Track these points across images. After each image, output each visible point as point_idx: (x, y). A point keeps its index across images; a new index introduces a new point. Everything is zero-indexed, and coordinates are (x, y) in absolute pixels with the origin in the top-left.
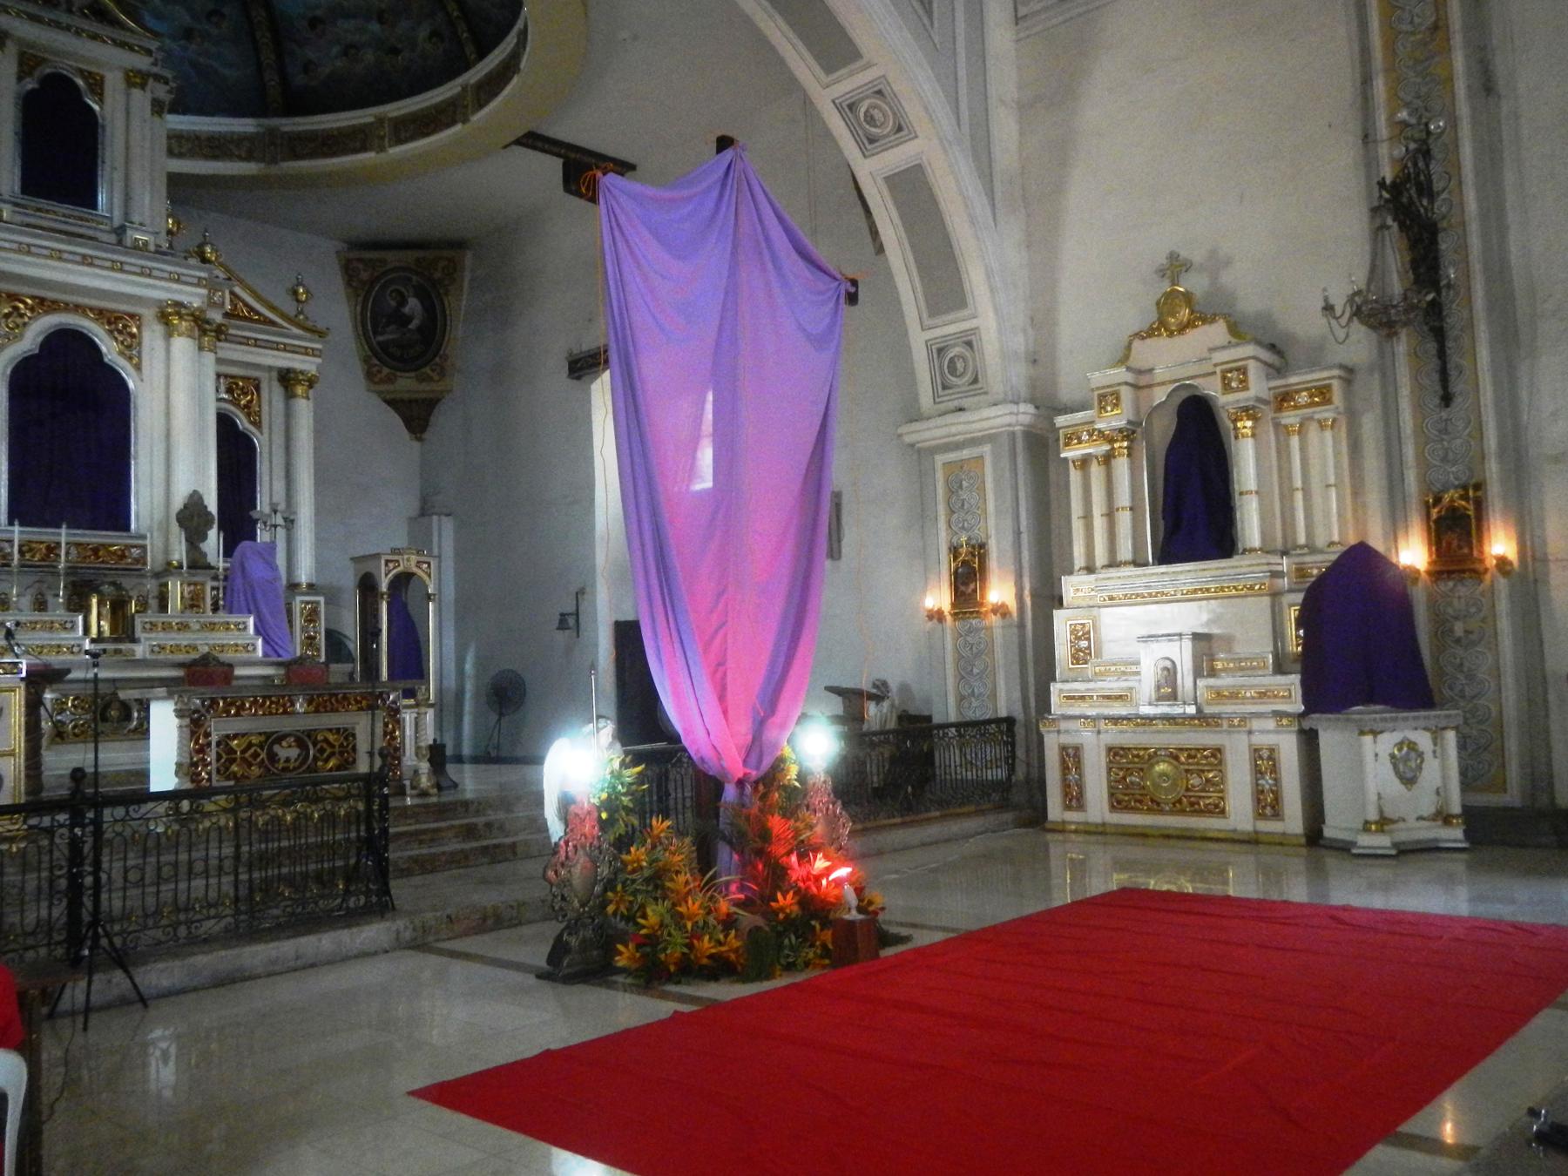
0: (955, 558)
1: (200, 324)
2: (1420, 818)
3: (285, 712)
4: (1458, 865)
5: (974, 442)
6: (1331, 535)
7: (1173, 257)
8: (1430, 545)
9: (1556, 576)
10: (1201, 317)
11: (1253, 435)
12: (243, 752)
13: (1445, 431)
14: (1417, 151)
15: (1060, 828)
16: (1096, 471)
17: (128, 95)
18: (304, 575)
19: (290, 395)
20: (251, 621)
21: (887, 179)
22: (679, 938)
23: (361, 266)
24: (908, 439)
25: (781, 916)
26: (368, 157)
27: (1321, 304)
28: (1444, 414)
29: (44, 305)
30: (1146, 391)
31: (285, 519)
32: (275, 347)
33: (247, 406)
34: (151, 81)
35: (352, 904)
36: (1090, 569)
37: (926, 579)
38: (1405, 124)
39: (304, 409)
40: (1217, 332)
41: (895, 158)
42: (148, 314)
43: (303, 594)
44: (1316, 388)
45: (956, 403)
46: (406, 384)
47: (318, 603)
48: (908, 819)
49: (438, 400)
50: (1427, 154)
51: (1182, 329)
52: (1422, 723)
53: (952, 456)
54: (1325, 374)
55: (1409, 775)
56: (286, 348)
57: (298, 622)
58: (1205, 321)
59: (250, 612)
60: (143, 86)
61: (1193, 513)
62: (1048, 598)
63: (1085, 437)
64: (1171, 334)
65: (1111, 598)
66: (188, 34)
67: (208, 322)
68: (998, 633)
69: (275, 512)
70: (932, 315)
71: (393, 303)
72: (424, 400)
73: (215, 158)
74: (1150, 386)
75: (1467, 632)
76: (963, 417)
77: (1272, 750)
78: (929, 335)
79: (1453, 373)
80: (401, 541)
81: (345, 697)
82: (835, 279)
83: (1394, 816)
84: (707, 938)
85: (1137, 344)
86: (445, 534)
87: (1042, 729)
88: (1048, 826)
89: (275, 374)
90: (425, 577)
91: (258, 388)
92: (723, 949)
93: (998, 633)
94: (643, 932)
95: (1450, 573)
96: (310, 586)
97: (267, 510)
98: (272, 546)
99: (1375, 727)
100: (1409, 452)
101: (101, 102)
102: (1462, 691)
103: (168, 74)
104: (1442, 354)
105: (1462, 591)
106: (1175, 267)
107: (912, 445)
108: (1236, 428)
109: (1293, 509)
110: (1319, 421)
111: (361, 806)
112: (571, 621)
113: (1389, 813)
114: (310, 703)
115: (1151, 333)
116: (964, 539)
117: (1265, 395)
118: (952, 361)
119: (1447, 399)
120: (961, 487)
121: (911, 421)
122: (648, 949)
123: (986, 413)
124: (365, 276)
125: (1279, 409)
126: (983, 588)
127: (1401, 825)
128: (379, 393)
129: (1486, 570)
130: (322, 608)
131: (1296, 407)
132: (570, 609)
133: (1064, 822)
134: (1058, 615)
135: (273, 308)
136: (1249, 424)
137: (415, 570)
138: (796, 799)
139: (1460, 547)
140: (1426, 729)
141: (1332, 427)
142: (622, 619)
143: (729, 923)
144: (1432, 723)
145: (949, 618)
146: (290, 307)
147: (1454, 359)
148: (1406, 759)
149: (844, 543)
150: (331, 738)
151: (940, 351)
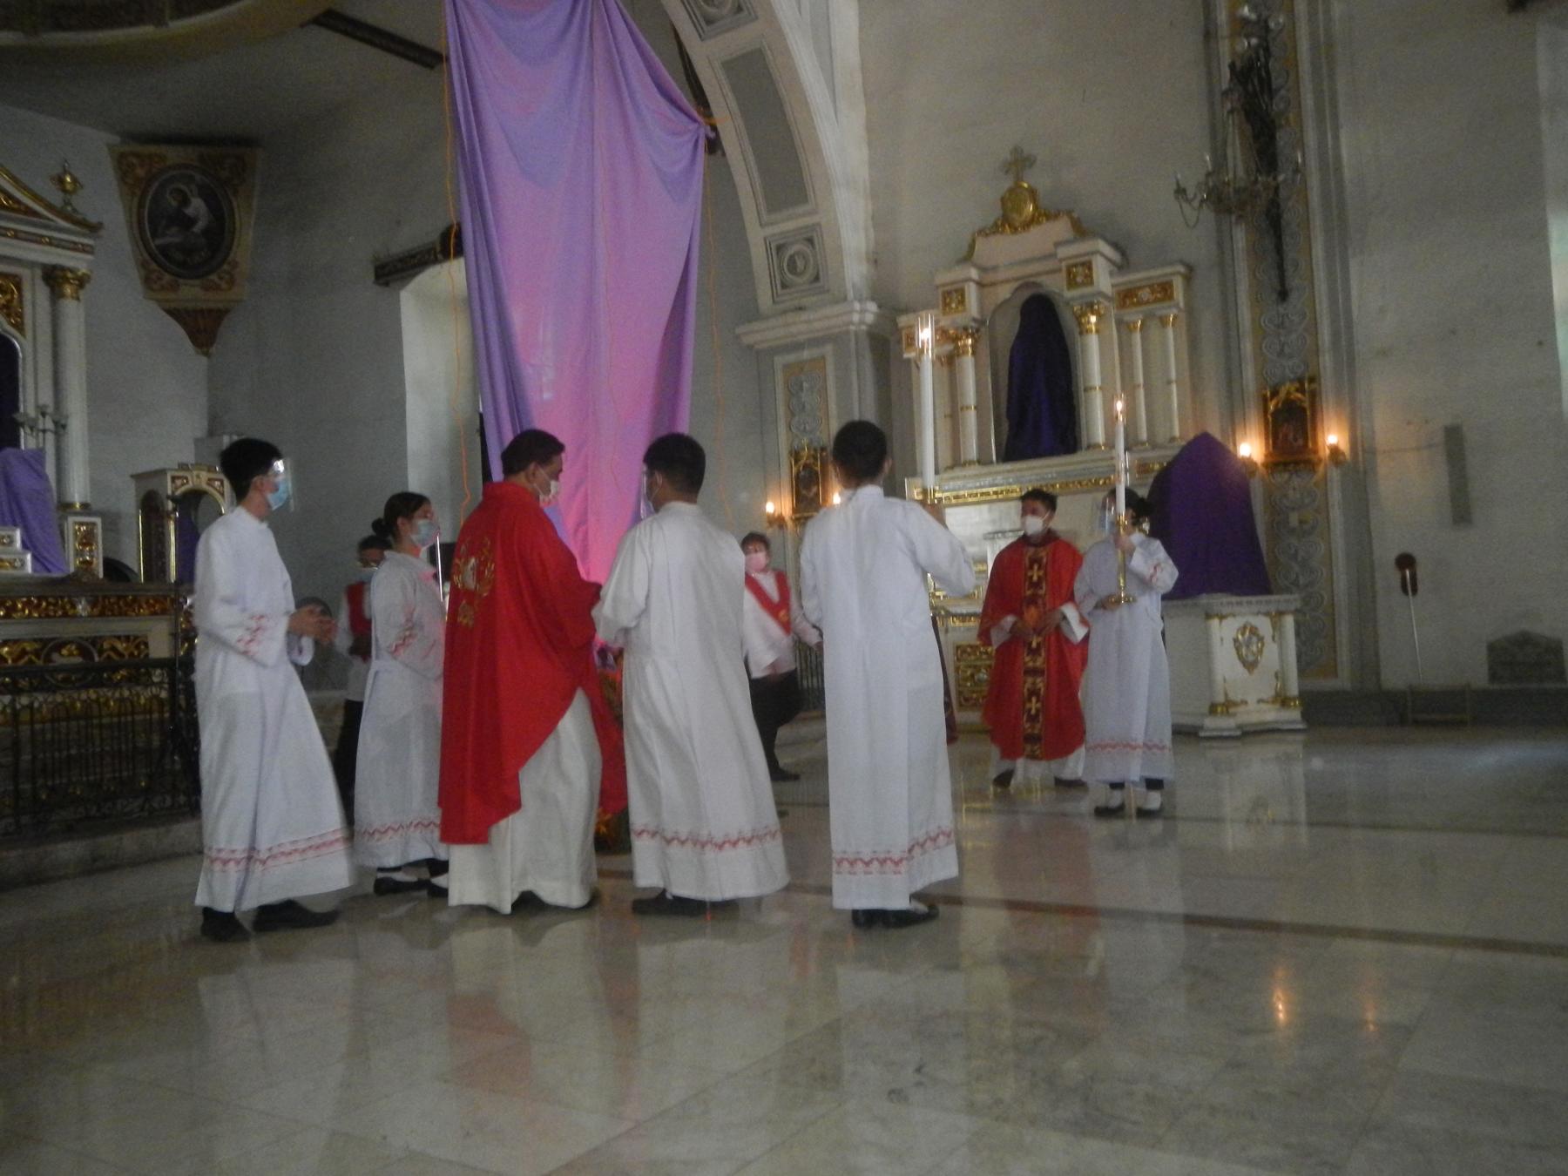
0: (796, 461)
2: (1260, 701)
3: (65, 615)
4: (1294, 746)
6: (1171, 428)
7: (1016, 150)
8: (1267, 439)
9: (1384, 468)
10: (1045, 215)
13: (1281, 325)
14: (1259, 46)
18: (78, 492)
19: (56, 295)
20: (18, 535)
23: (135, 161)
24: (747, 340)
26: (148, 30)
28: (1281, 310)
30: (986, 290)
31: (56, 423)
32: (37, 239)
35: (156, 805)
38: (1245, 21)
39: (73, 311)
43: (76, 514)
45: (796, 303)
46: (191, 293)
47: (94, 524)
49: (227, 311)
50: (1267, 50)
51: (1027, 225)
52: (1264, 608)
53: (791, 358)
54: (1168, 270)
55: (1251, 658)
56: (52, 242)
57: (72, 545)
59: (15, 525)
64: (1015, 230)
65: (957, 497)
69: (44, 415)
70: (770, 211)
71: (174, 203)
72: (210, 311)
74: (993, 284)
75: (1301, 522)
76: (804, 316)
78: (769, 231)
80: (190, 458)
81: (135, 600)
82: (695, 121)
83: (1238, 698)
85: (980, 244)
89: (39, 272)
90: (218, 496)
95: (1286, 464)
96: (85, 506)
97: (32, 412)
98: (39, 455)
99: (1225, 611)
100: (1248, 347)
104: (1279, 250)
105: (1296, 481)
106: (1019, 162)
107: (750, 347)
108: (1080, 324)
111: (164, 694)
113: (1232, 696)
114: (93, 605)
115: (996, 229)
116: (805, 441)
118: (792, 260)
119: (1283, 295)
121: (750, 321)
123: (828, 311)
124: (140, 172)
126: (825, 492)
127: (1241, 709)
128: (158, 301)
129: (1320, 460)
130: (99, 531)
131: (1140, 303)
135: (36, 197)
137: (205, 487)
139: (1296, 440)
140: (1267, 614)
144: (1273, 609)
145: (790, 524)
146: (56, 198)
147: (1290, 254)
150: (121, 646)
151: (780, 248)
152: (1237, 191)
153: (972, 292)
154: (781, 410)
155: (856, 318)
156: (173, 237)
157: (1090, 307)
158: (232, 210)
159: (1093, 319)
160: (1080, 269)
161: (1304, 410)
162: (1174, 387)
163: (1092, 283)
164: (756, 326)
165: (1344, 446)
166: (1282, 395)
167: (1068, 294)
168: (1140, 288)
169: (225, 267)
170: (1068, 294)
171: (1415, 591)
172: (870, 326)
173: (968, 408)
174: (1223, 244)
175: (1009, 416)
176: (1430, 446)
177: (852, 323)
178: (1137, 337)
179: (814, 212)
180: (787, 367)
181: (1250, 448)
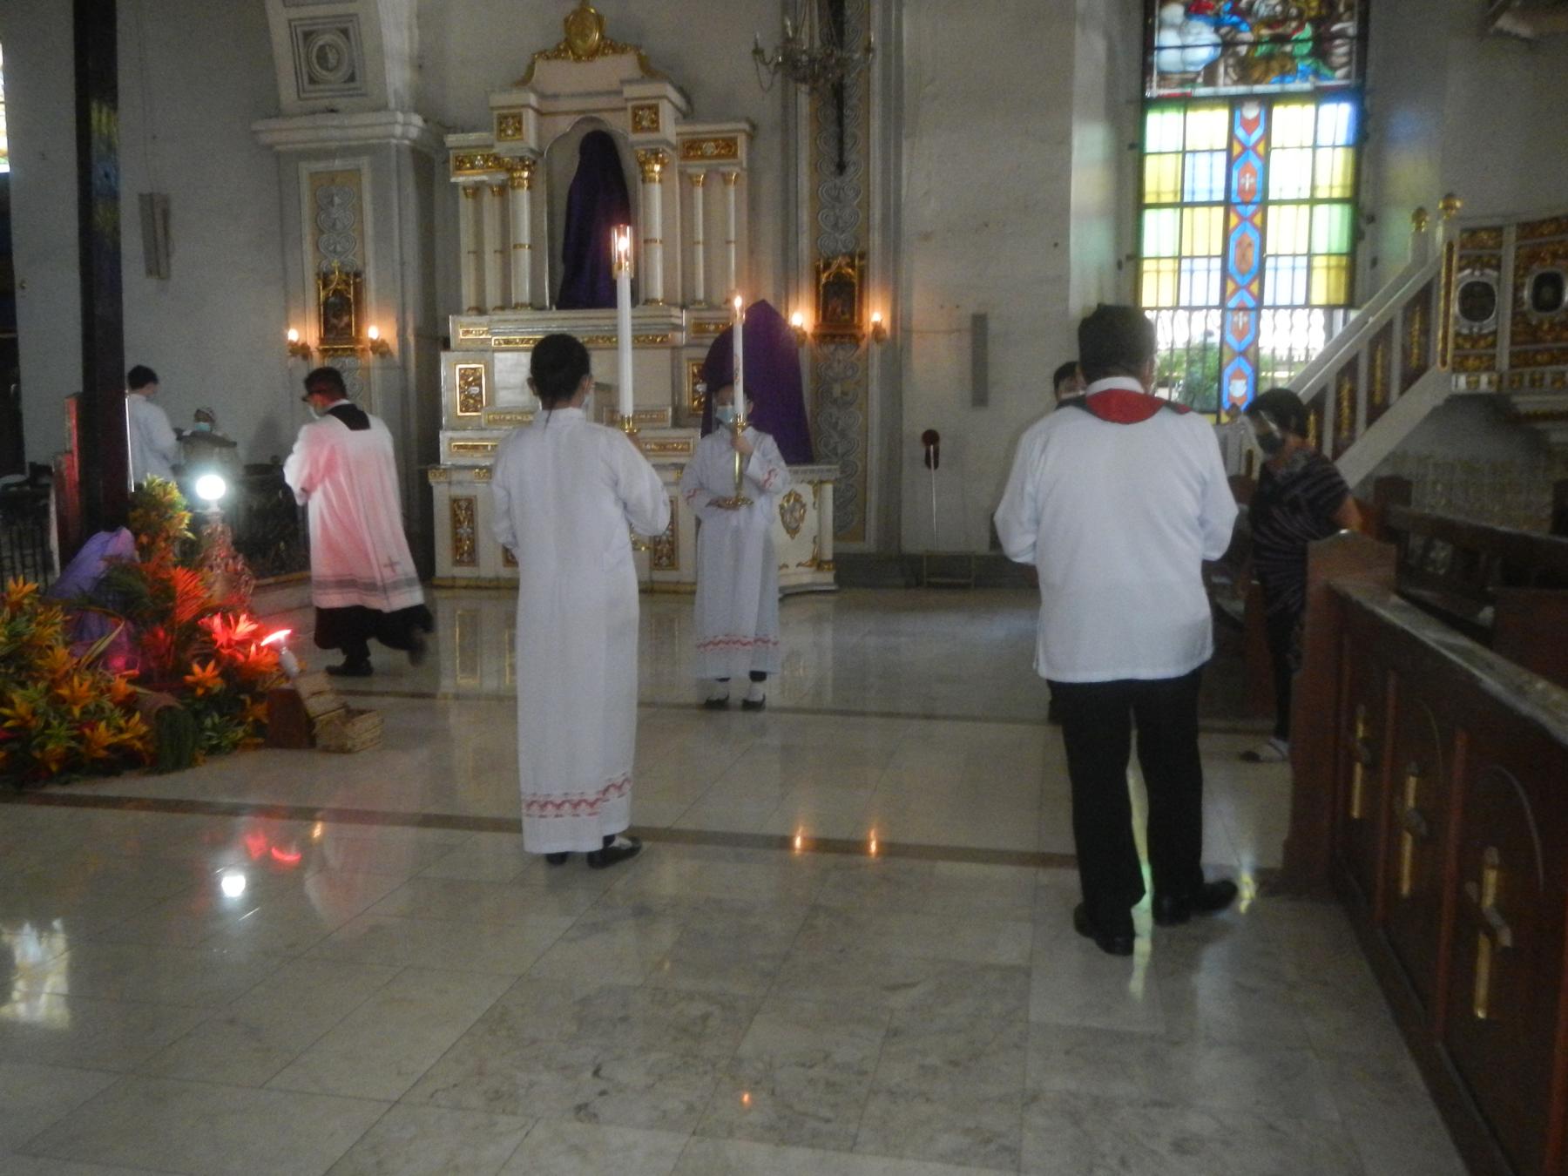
0: (325, 287)
10: (611, 46)
11: (661, 181)
15: (451, 585)
16: (490, 202)
22: (60, 730)
24: (266, 139)
25: (200, 691)
27: (752, 47)
28: (838, 181)
36: (480, 310)
37: (286, 310)
40: (626, 65)
45: (326, 102)
48: (283, 578)
51: (593, 54)
52: (809, 477)
53: (320, 166)
55: (794, 525)
58: (615, 51)
62: (434, 341)
63: (479, 161)
64: (578, 59)
65: (507, 342)
68: (376, 375)
75: (844, 393)
76: (334, 120)
79: (848, 141)
84: (102, 725)
85: (541, 65)
87: (432, 480)
88: (436, 582)
92: (126, 736)
93: (376, 375)
94: (8, 724)
100: (805, 216)
102: (835, 448)
105: (841, 354)
107: (270, 147)
108: (643, 172)
109: (693, 262)
110: (723, 175)
115: (556, 54)
116: (335, 264)
117: (674, 140)
118: (322, 48)
119: (841, 167)
120: (331, 203)
122: (16, 746)
125: (685, 157)
131: (703, 157)
133: (454, 578)
134: (444, 356)
136: (657, 168)
138: (192, 553)
139: (843, 313)
140: (810, 482)
143: (129, 705)
144: (816, 478)
145: (316, 355)
147: (850, 128)
148: (792, 511)
149: (172, 261)
151: (307, 35)
152: (812, 61)
153: (530, 118)
154: (307, 229)
155: (398, 130)
159: (657, 168)
160: (647, 112)
161: (852, 285)
162: (733, 246)
163: (657, 129)
164: (273, 123)
165: (886, 325)
166: (834, 267)
167: (633, 137)
168: (705, 141)
170: (634, 137)
171: (936, 466)
172: (414, 141)
173: (522, 246)
174: (787, 107)
175: (565, 258)
176: (959, 330)
177: (394, 137)
178: (699, 191)
181: (801, 318)
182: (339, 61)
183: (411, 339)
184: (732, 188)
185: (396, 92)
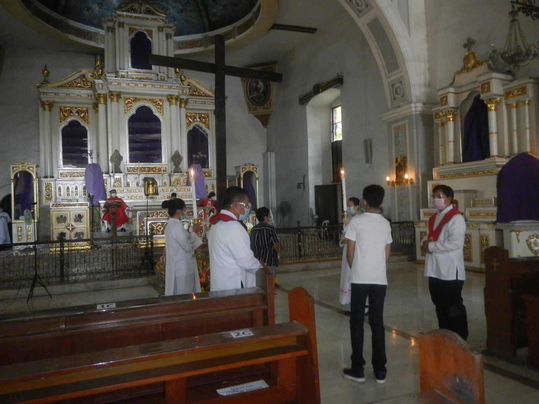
1: (177, 99)
5: (403, 119)
7: (469, 39)
10: (478, 64)
11: (495, 110)
12: (157, 227)
17: (158, 34)
21: (369, 25)
29: (136, 100)
30: (460, 95)
33: (205, 122)
34: (164, 29)
40: (484, 68)
41: (368, 17)
42: (165, 99)
44: (521, 88)
46: (260, 110)
53: (396, 125)
58: (479, 64)
60: (162, 31)
61: (476, 143)
62: (428, 176)
66: (181, 11)
67: (183, 99)
68: (410, 189)
70: (389, 72)
71: (255, 85)
73: (191, 47)
74: (461, 93)
76: (399, 110)
77: (487, 237)
86: (272, 156)
91: (208, 117)
93: (410, 189)
101: (152, 38)
103: (171, 25)
106: (469, 44)
107: (385, 121)
112: (302, 186)
118: (396, 89)
126: (405, 174)
132: (301, 181)
141: (528, 104)
142: (317, 184)
149: (373, 158)
151: (392, 85)
155: (413, 109)
156: (255, 95)
157: (490, 101)
158: (270, 85)
160: (486, 85)
163: (490, 91)
169: (269, 101)
172: (421, 111)
173: (450, 142)
178: (514, 110)
179: (401, 72)
180: (395, 128)
182: (400, 92)
183: (420, 177)
184: (527, 108)
185: (416, 97)
